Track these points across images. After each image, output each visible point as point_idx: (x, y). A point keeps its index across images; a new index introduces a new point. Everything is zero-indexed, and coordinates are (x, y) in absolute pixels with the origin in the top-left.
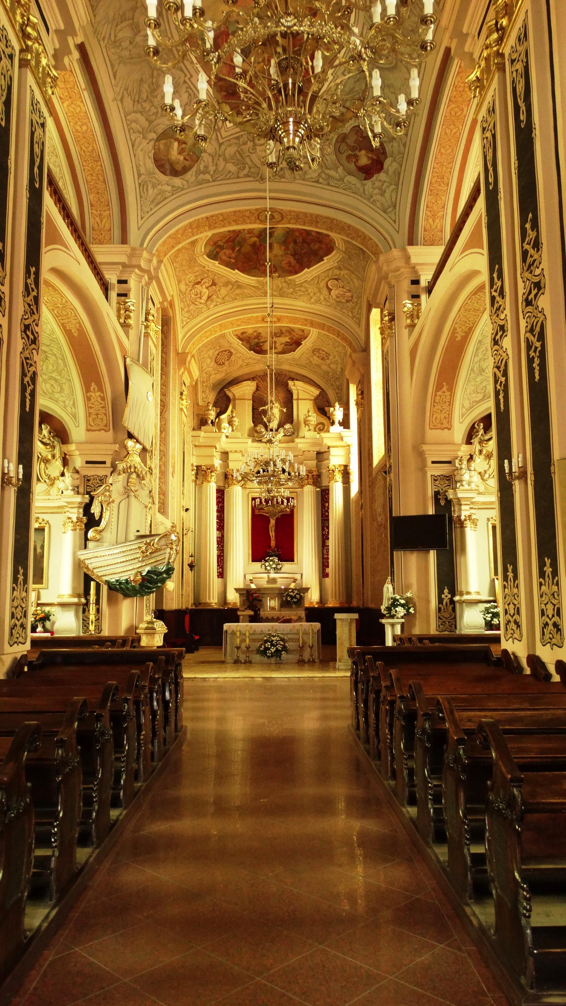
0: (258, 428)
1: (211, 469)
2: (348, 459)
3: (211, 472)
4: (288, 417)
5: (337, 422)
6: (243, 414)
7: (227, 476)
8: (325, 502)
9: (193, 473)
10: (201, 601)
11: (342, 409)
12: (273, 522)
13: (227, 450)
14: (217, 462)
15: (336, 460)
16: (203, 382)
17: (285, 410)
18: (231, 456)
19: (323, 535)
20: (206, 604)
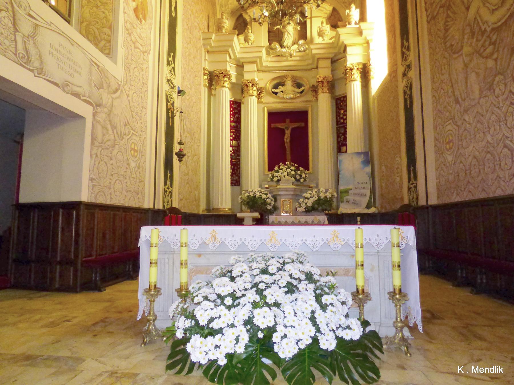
0: (273, 45)
1: (226, 75)
2: (368, 57)
3: (224, 76)
4: (303, 34)
5: (353, 23)
6: (259, 35)
7: (242, 88)
8: (340, 109)
9: (206, 77)
10: (215, 207)
11: (358, 10)
12: (288, 133)
13: (242, 60)
14: (232, 71)
15: (354, 58)
16: (222, 6)
17: (299, 28)
18: (247, 67)
19: (338, 142)
20: (218, 209)
